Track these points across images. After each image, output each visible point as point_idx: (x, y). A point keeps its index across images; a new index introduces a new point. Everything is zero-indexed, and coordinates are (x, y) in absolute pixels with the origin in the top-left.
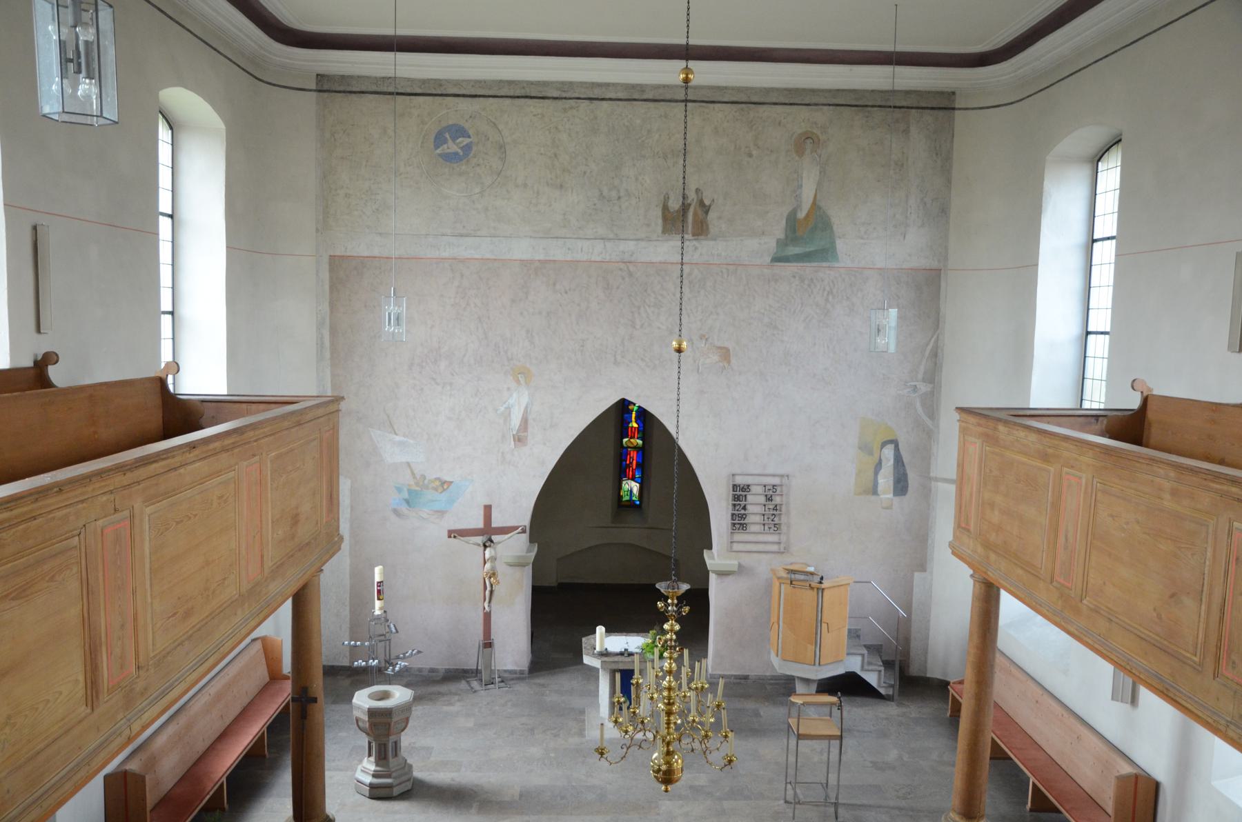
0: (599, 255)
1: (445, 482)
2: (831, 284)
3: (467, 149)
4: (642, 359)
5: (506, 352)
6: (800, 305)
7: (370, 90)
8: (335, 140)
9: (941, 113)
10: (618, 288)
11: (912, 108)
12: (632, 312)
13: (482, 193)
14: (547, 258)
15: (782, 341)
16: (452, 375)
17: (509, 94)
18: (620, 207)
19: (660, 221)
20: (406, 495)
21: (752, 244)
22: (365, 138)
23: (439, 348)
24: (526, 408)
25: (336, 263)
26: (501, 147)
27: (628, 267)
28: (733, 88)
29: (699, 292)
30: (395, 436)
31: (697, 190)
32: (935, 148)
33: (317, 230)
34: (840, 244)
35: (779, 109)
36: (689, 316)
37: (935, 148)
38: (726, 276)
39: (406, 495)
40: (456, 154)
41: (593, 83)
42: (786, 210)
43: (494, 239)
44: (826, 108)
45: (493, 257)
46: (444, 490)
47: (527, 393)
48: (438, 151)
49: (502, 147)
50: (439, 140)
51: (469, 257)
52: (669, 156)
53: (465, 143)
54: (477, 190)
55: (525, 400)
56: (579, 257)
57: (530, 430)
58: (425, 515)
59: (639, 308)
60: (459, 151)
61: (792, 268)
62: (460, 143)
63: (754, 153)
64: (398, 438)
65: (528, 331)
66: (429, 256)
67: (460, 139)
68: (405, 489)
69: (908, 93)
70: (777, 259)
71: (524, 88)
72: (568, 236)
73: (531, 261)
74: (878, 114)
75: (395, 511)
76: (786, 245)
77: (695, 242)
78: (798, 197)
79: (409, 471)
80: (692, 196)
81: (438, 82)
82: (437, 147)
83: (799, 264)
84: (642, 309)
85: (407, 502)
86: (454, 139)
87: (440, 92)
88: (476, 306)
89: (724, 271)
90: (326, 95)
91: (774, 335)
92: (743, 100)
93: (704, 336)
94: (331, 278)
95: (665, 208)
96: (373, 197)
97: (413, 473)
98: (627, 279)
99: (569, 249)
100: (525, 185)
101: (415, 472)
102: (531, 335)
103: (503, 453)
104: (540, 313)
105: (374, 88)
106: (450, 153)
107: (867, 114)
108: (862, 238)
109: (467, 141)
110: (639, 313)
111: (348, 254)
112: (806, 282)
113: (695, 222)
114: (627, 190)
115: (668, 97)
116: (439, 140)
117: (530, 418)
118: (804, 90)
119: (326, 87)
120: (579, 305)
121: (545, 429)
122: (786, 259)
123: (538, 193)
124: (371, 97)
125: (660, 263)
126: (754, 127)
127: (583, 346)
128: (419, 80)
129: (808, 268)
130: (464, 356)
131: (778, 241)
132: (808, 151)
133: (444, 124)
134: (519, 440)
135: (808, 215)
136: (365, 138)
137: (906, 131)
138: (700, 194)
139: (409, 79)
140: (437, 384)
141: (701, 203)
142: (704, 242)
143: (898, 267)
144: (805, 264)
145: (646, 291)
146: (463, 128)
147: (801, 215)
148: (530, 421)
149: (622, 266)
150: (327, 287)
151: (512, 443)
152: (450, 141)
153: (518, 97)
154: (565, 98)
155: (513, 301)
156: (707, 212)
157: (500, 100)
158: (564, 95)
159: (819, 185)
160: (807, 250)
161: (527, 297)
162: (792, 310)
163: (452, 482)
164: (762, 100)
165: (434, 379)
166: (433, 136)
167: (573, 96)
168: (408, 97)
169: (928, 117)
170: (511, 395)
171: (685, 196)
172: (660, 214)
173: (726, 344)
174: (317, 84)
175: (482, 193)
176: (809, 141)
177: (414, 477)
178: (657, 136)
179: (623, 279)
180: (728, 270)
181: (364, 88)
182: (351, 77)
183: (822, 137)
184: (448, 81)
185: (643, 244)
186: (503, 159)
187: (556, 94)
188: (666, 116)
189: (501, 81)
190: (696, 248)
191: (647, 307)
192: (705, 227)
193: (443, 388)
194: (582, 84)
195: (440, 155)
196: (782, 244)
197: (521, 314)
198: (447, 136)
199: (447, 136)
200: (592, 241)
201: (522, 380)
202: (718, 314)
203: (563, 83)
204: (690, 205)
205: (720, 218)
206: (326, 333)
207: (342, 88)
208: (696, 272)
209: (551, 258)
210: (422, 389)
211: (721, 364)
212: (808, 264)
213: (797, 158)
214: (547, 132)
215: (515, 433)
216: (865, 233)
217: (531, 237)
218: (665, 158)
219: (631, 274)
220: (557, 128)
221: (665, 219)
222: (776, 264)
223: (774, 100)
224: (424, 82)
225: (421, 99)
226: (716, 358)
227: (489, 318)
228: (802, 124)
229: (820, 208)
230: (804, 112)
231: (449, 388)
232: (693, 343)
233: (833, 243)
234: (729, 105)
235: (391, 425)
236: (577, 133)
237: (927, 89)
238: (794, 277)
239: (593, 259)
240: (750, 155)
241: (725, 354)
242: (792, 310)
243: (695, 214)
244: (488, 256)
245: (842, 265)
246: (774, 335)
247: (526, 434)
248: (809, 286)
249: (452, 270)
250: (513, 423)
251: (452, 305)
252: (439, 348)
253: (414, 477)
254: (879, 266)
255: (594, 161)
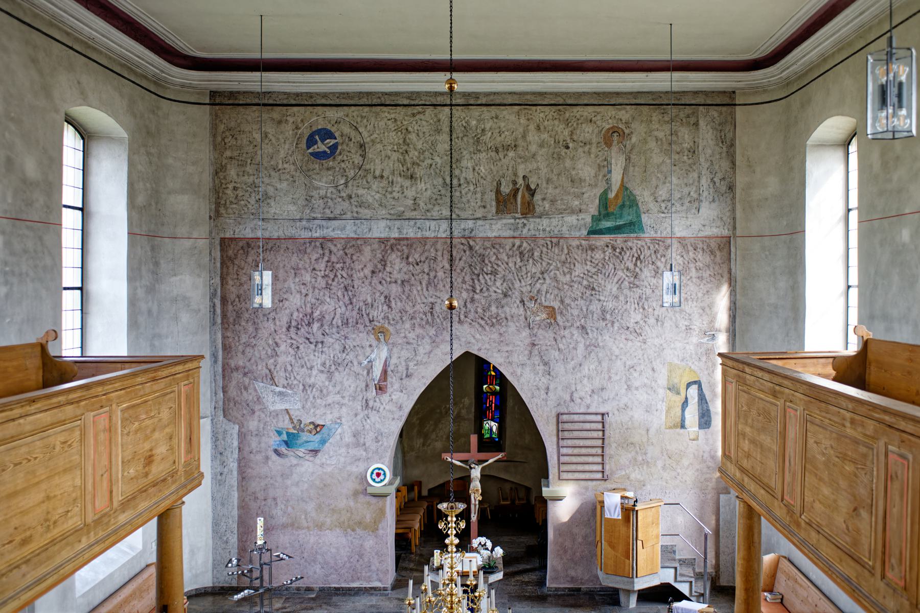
0: (444, 232)
1: (318, 425)
2: (639, 252)
3: (334, 148)
4: (482, 318)
5: (368, 315)
6: (613, 270)
7: (254, 102)
8: (225, 144)
9: (724, 109)
10: (460, 259)
11: (700, 105)
12: (473, 279)
13: (346, 184)
14: (401, 236)
15: (600, 300)
16: (323, 335)
17: (367, 103)
18: (461, 192)
19: (494, 203)
20: (285, 437)
21: (572, 219)
22: (250, 141)
23: (312, 312)
24: (386, 361)
25: (225, 243)
26: (361, 146)
27: (468, 243)
28: (551, 94)
29: (528, 261)
30: (275, 387)
31: (524, 177)
32: (721, 137)
33: (210, 217)
34: (645, 218)
35: (590, 109)
36: (520, 281)
37: (721, 137)
38: (550, 247)
39: (285, 437)
40: (325, 152)
41: (436, 92)
42: (599, 191)
43: (357, 221)
44: (628, 107)
45: (356, 236)
46: (317, 432)
47: (386, 349)
48: (310, 150)
49: (362, 146)
50: (311, 142)
51: (336, 236)
52: (500, 150)
53: (331, 144)
54: (342, 181)
55: (384, 354)
56: (428, 234)
57: (389, 379)
58: (301, 454)
59: (479, 275)
60: (327, 150)
61: (606, 238)
62: (327, 143)
63: (571, 145)
64: (278, 389)
65: (386, 297)
66: (303, 237)
67: (328, 141)
68: (284, 432)
69: (696, 93)
70: (592, 232)
71: (379, 98)
72: (418, 217)
73: (388, 239)
74: (674, 111)
75: (276, 451)
76: (600, 220)
77: (523, 220)
78: (608, 181)
79: (287, 417)
80: (520, 181)
81: (310, 95)
82: (308, 148)
83: (612, 236)
84: (481, 276)
85: (286, 443)
86: (323, 141)
87: (310, 103)
88: (342, 277)
89: (549, 243)
90: (217, 107)
91: (592, 295)
92: (561, 103)
93: (534, 297)
94: (222, 256)
95: (498, 192)
96: (256, 189)
97: (291, 419)
98: (468, 252)
99: (419, 228)
100: (382, 177)
101: (293, 417)
102: (389, 300)
103: (366, 400)
104: (396, 282)
105: (256, 101)
106: (319, 152)
107: (662, 111)
108: (663, 213)
109: (333, 142)
110: (479, 280)
111: (236, 236)
112: (618, 250)
113: (523, 203)
114: (466, 179)
115: (498, 102)
116: (311, 142)
117: (389, 370)
118: (610, 93)
119: (217, 101)
120: (428, 274)
121: (401, 379)
122: (600, 232)
123: (392, 182)
124: (255, 108)
125: (495, 237)
126: (570, 124)
127: (432, 308)
128: (294, 94)
129: (619, 239)
130: (333, 319)
131: (593, 216)
132: (615, 143)
133: (314, 129)
134: (380, 389)
135: (617, 195)
136: (250, 141)
137: (696, 124)
138: (527, 179)
139: (285, 93)
140: (311, 343)
141: (528, 187)
142: (531, 220)
143: (694, 236)
144: (616, 236)
145: (484, 261)
146: (330, 131)
147: (612, 195)
148: (389, 373)
149: (463, 241)
150: (218, 265)
151: (374, 391)
152: (319, 142)
153: (375, 105)
154: (414, 105)
155: (373, 272)
156: (533, 195)
157: (361, 108)
158: (413, 102)
159: (625, 170)
160: (618, 224)
161: (384, 269)
162: (607, 274)
163: (324, 426)
164: (575, 102)
165: (308, 339)
166: (306, 138)
167: (420, 103)
168: (285, 108)
169: (714, 112)
170: (373, 351)
171: (515, 183)
172: (494, 197)
173: (552, 304)
174: (210, 99)
175: (346, 184)
176: (615, 135)
177: (293, 422)
178: (490, 134)
179: (465, 251)
180: (551, 241)
181: (248, 101)
182: (238, 92)
183: (627, 131)
184: (317, 94)
185: (480, 222)
186: (363, 156)
187: (406, 102)
188: (497, 118)
189: (360, 93)
190: (525, 225)
191: (485, 275)
192: (531, 208)
193: (316, 346)
194: (428, 94)
195: (311, 154)
196: (596, 219)
197: (380, 282)
198: (317, 137)
199: (317, 137)
200: (438, 221)
201: (382, 338)
202: (544, 279)
203: (412, 93)
204: (518, 189)
205: (544, 199)
206: (218, 302)
207: (231, 102)
208: (525, 245)
209: (404, 236)
210: (298, 348)
211: (549, 321)
212: (619, 236)
213: (606, 149)
214: (400, 133)
215: (376, 382)
216: (666, 208)
217: (387, 219)
218: (497, 151)
219: (471, 248)
220: (407, 129)
221: (498, 201)
222: (591, 236)
223: (586, 102)
224: (297, 95)
225: (295, 109)
226: (544, 316)
227: (353, 287)
228: (610, 121)
229: (627, 189)
230: (611, 111)
231: (320, 345)
232: (524, 304)
233: (639, 216)
234: (549, 107)
235: (272, 379)
236: (424, 133)
237: (713, 90)
238: (607, 246)
239: (439, 236)
240: (567, 147)
241: (552, 313)
242: (607, 274)
243: (523, 197)
244: (353, 235)
245: (647, 235)
246: (592, 295)
247: (385, 383)
248: (620, 253)
249: (322, 247)
250: (374, 374)
251: (323, 277)
252: (312, 312)
253: (293, 422)
254: (678, 235)
255: (438, 156)
